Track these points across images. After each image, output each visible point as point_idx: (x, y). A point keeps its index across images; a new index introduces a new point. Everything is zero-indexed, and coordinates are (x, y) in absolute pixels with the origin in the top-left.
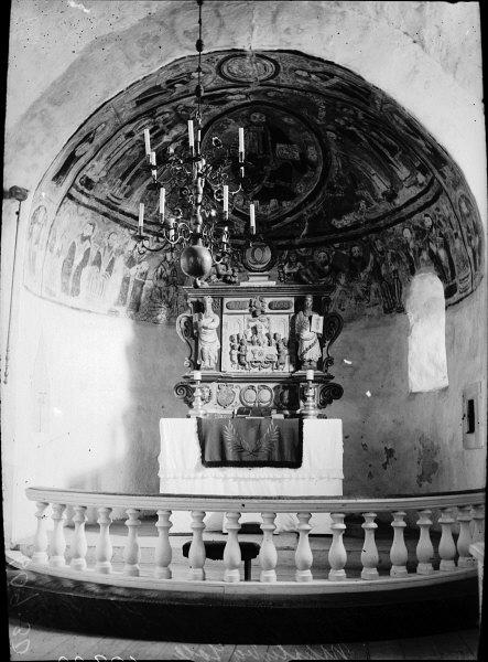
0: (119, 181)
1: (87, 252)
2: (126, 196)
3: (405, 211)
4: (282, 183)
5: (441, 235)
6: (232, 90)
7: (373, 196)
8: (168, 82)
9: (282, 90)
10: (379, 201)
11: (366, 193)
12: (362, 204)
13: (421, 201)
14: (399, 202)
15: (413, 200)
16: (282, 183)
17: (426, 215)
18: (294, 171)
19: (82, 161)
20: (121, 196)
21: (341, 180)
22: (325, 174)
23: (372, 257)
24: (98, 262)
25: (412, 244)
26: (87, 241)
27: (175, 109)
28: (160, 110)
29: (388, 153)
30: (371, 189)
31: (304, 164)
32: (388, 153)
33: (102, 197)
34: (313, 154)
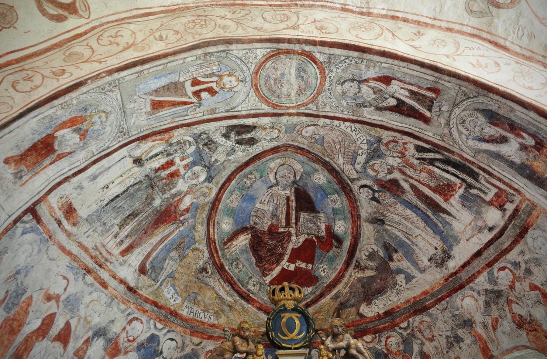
0: (116, 229)
1: (49, 320)
2: (125, 252)
3: (464, 276)
4: (303, 265)
5: (533, 288)
6: (266, 121)
7: (415, 264)
8: (195, 82)
9: (321, 121)
10: (422, 271)
11: (405, 264)
12: (400, 279)
13: (490, 253)
14: (453, 265)
15: (478, 254)
16: (303, 265)
17: (503, 269)
18: (318, 251)
19: (63, 167)
20: (116, 252)
21: (372, 256)
22: (352, 252)
23: (416, 348)
24: (64, 337)
25: (478, 318)
26: (53, 302)
27: (197, 137)
28: (178, 135)
29: (438, 198)
30: (410, 255)
31: (332, 239)
32: (438, 198)
33: (88, 243)
34: (341, 227)
